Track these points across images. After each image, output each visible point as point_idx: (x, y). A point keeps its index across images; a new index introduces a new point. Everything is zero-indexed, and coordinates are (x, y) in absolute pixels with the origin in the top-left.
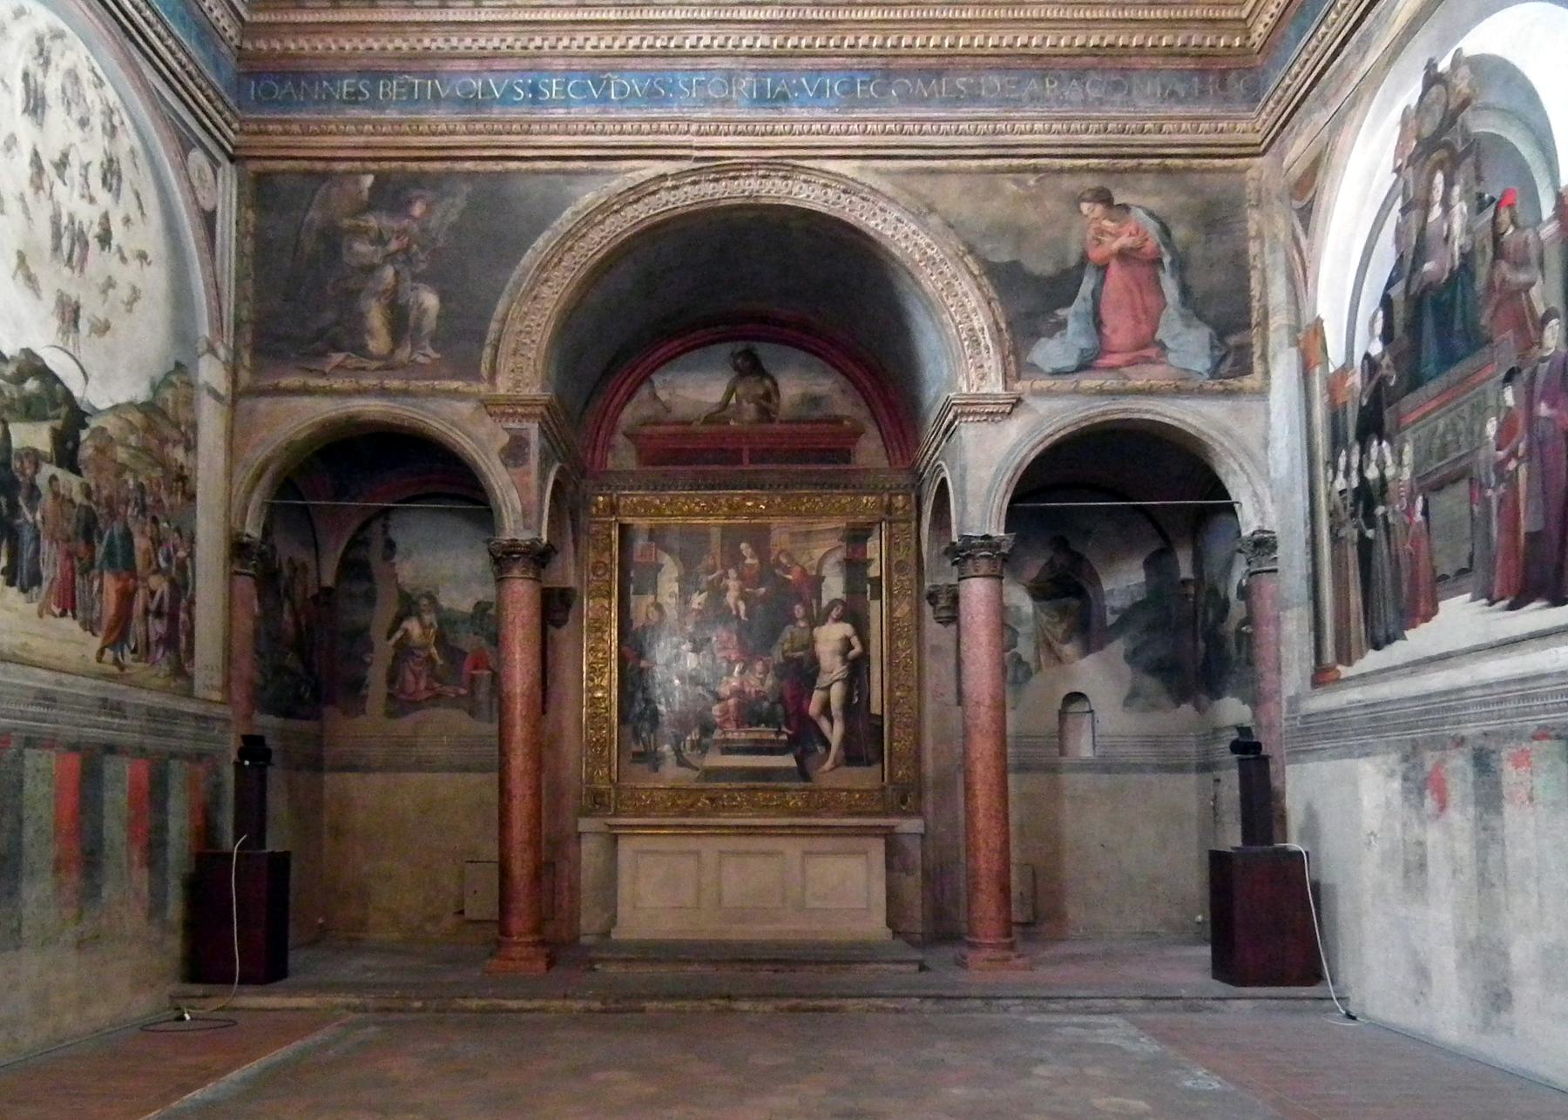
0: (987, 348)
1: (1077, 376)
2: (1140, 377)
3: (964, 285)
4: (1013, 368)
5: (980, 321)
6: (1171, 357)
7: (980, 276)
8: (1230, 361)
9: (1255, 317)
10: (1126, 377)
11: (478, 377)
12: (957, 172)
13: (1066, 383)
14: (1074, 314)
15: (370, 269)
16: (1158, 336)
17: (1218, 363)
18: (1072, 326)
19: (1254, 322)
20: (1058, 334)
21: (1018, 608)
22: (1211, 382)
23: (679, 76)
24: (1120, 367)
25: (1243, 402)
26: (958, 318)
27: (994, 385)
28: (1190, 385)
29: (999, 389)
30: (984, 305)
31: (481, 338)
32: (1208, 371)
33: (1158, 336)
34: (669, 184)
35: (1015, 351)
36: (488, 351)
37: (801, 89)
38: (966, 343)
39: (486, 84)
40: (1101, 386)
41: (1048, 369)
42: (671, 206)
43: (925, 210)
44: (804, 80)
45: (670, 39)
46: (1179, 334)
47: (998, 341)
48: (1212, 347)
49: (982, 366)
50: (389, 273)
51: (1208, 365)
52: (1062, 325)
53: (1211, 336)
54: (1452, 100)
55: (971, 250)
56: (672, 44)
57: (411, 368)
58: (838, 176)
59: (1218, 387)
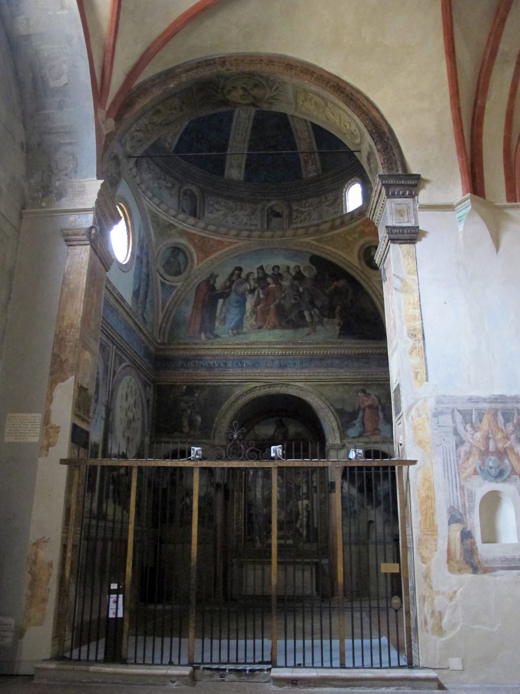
2: (374, 438)
3: (330, 414)
4: (343, 436)
5: (334, 424)
6: (382, 433)
11: (209, 438)
12: (328, 385)
13: (357, 440)
14: (357, 422)
15: (184, 410)
18: (357, 425)
27: (338, 442)
29: (339, 442)
33: (379, 427)
34: (258, 388)
36: (213, 432)
37: (290, 363)
41: (351, 436)
52: (354, 425)
58: (299, 387)
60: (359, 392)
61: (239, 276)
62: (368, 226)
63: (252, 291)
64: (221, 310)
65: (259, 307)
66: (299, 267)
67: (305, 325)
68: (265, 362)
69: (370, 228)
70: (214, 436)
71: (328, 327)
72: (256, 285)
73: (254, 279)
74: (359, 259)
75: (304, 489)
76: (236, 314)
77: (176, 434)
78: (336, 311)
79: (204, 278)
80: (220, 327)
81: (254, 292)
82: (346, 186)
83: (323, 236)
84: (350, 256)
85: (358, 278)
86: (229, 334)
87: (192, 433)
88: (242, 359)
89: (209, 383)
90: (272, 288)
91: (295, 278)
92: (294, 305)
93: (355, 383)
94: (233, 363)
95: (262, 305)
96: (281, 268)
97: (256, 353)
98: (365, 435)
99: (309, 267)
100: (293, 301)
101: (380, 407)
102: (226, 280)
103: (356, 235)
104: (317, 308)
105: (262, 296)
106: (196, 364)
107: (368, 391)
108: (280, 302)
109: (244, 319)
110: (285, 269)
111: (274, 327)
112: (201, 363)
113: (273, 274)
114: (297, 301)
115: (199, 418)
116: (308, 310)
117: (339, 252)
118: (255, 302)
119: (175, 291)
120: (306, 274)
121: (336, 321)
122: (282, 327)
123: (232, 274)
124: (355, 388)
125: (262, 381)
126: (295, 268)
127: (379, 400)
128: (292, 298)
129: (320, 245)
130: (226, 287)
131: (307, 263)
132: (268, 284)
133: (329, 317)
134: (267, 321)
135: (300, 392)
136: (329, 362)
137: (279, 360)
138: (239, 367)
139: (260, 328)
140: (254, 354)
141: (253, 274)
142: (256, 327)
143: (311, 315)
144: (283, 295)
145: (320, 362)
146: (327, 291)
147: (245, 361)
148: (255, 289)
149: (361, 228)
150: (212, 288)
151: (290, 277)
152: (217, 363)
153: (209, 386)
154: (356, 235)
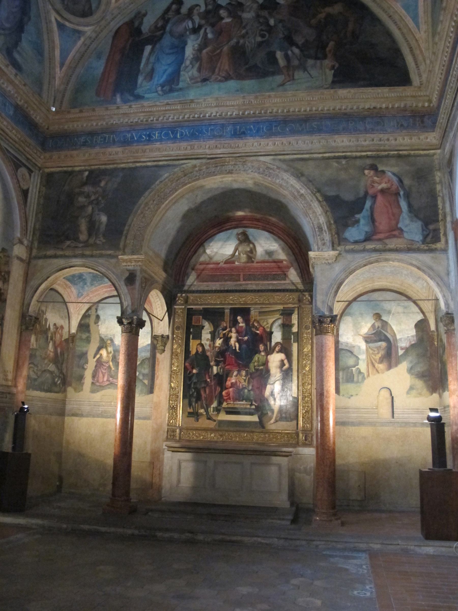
5: (322, 220)
6: (405, 235)
7: (323, 201)
9: (440, 217)
14: (363, 217)
15: (83, 207)
16: (400, 225)
17: (425, 237)
18: (362, 222)
19: (440, 219)
20: (356, 226)
21: (359, 347)
22: (423, 246)
23: (204, 127)
25: (438, 255)
26: (313, 219)
28: (414, 247)
30: (324, 214)
31: (121, 233)
32: (421, 241)
33: (400, 225)
35: (338, 233)
36: (123, 238)
37: (251, 130)
38: (317, 230)
39: (132, 135)
40: (375, 248)
41: (352, 241)
42: (197, 177)
43: (300, 175)
44: (252, 126)
45: (201, 114)
46: (409, 225)
48: (423, 230)
49: (323, 240)
50: (90, 209)
51: (421, 238)
52: (358, 221)
53: (422, 225)
55: (319, 191)
56: (201, 116)
57: (95, 246)
59: (426, 248)
60: (364, 169)
61: (178, 12)
63: (195, 31)
64: (148, 59)
65: (204, 51)
67: (277, 71)
68: (211, 130)
70: (125, 246)
71: (314, 72)
72: (203, 22)
73: (199, 14)
75: (277, 337)
76: (169, 64)
77: (68, 243)
78: (328, 49)
79: (127, 19)
80: (145, 83)
81: (199, 32)
86: (157, 92)
87: (91, 241)
88: (175, 128)
89: (123, 166)
90: (226, 23)
92: (260, 44)
93: (358, 154)
94: (161, 133)
95: (209, 48)
97: (196, 116)
98: (375, 237)
100: (259, 39)
101: (402, 193)
102: (159, 18)
104: (298, 47)
105: (210, 36)
106: (105, 138)
107: (380, 168)
109: (181, 69)
111: (227, 78)
112: (113, 137)
113: (229, 4)
114: (264, 39)
115: (104, 219)
118: (199, 45)
119: (82, 39)
122: (240, 77)
123: (168, 10)
124: (358, 162)
125: (203, 156)
127: (401, 181)
130: (157, 28)
132: (222, 19)
133: (317, 58)
134: (217, 70)
135: (266, 171)
136: (314, 124)
137: (234, 124)
138: (169, 139)
139: (205, 80)
140: (194, 117)
141: (198, 8)
142: (199, 80)
144: (244, 31)
145: (301, 125)
146: (313, 22)
147: (179, 129)
148: (200, 27)
150: (138, 31)
151: (255, 6)
152: (136, 136)
153: (123, 169)
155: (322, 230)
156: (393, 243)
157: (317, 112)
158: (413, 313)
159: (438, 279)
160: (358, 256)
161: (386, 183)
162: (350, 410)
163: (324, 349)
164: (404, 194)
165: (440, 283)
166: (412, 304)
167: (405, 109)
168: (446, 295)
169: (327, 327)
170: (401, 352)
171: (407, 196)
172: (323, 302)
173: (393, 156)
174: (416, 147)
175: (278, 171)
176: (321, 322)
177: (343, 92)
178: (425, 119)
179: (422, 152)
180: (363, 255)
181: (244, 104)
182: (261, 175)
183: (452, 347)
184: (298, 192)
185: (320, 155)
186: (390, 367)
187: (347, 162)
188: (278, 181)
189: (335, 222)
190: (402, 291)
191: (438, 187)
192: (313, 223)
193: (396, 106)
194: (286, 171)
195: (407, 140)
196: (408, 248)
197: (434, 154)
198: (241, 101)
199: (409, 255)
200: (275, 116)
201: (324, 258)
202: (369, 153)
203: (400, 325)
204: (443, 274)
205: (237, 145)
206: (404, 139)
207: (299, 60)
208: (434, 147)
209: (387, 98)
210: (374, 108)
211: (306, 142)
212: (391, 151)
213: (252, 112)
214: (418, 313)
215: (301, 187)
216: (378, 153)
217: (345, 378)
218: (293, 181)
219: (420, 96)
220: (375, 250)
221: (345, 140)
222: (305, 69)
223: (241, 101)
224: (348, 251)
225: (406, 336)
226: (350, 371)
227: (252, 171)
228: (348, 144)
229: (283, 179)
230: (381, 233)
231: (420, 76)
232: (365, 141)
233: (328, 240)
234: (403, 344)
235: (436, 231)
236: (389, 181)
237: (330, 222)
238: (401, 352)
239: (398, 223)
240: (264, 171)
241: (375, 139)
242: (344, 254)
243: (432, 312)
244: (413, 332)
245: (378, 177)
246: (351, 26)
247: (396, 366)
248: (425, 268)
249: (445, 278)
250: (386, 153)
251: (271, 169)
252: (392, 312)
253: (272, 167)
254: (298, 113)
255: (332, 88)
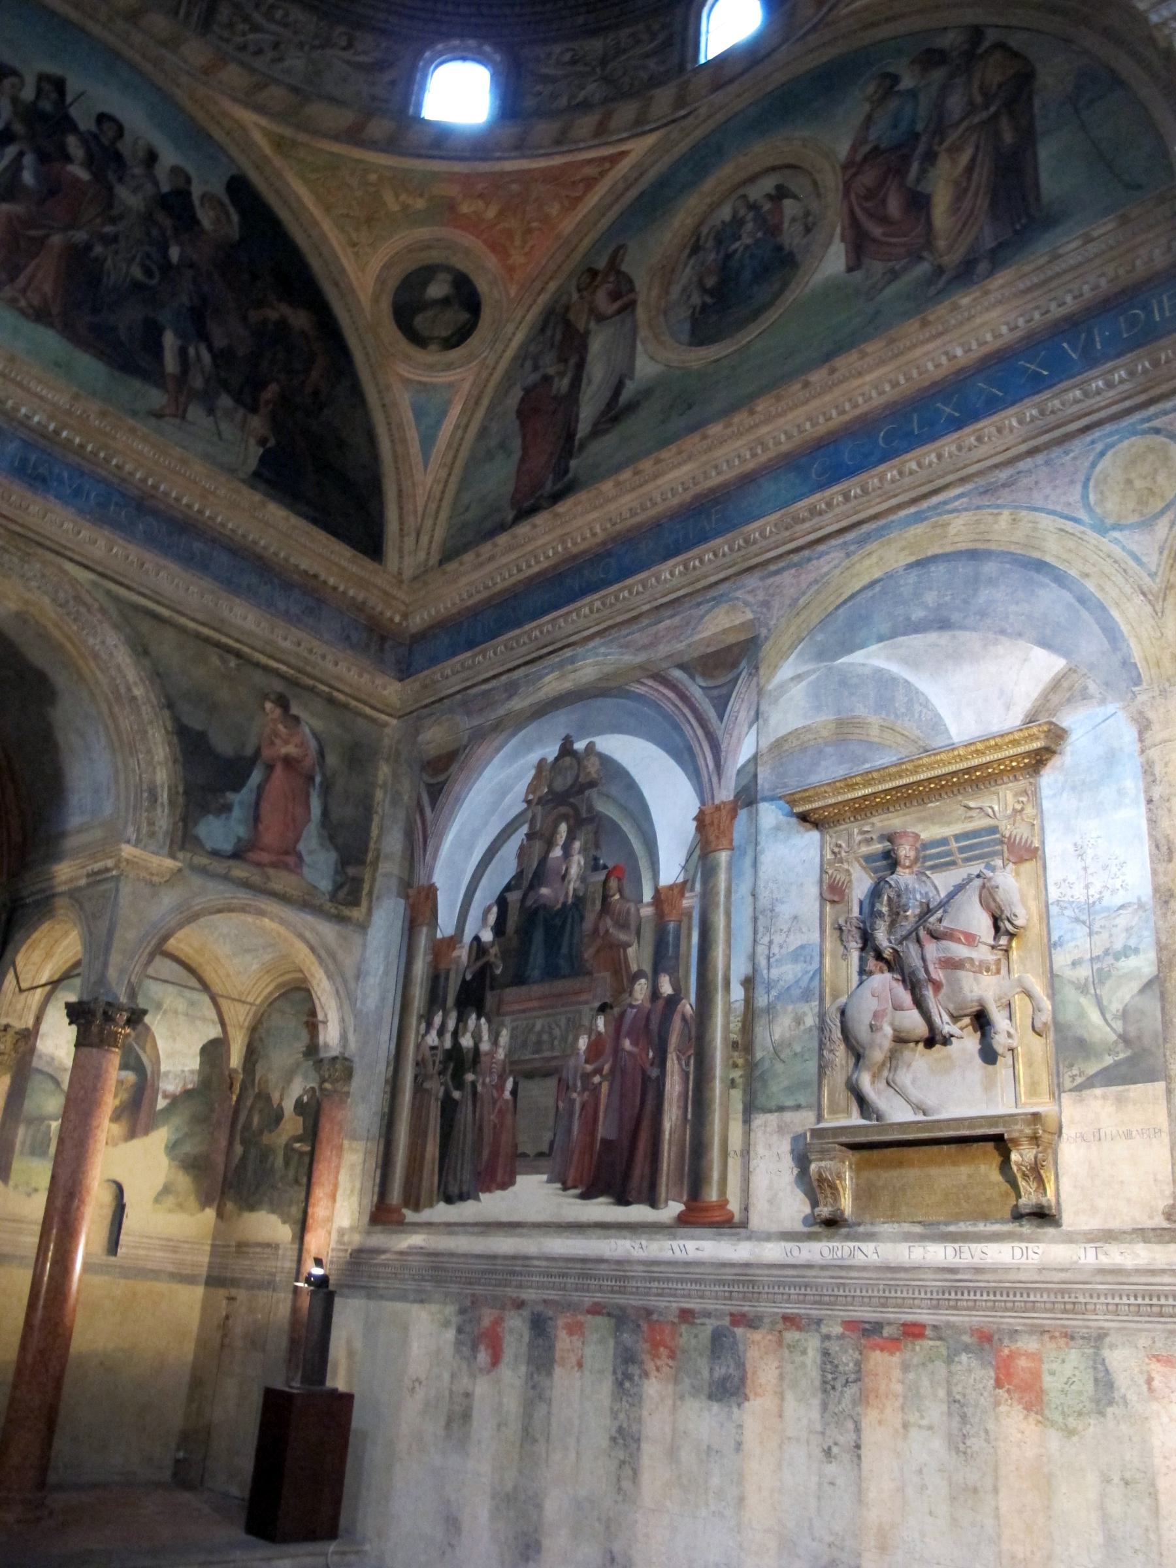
0: (162, 805)
1: (231, 862)
5: (162, 776)
6: (306, 870)
8: (345, 889)
10: (268, 878)
13: (218, 866)
14: (240, 799)
17: (338, 887)
18: (237, 813)
20: (224, 816)
22: (329, 904)
24: (265, 865)
26: (143, 765)
33: (301, 847)
35: (185, 819)
37: (60, 481)
40: (247, 878)
41: (209, 845)
43: (140, 649)
44: (66, 474)
47: (172, 802)
48: (337, 872)
49: (154, 824)
51: (330, 888)
52: (227, 808)
54: (582, 775)
55: (170, 705)
59: (333, 911)
60: (266, 697)
62: (481, 196)
66: (188, 180)
67: (153, 375)
69: (480, 204)
71: (224, 426)
74: (381, 281)
82: (440, 47)
83: (302, 137)
84: (357, 254)
85: (352, 342)
91: (164, 202)
92: (137, 286)
93: (264, 660)
96: (128, 138)
98: (254, 856)
99: (222, 204)
100: (137, 272)
101: (318, 779)
103: (420, 204)
104: (210, 349)
107: (295, 710)
108: (88, 247)
110: (141, 154)
111: (40, 316)
113: (95, 137)
116: (180, 334)
117: (327, 225)
120: (206, 218)
121: (257, 423)
124: (258, 677)
126: (176, 171)
127: (321, 754)
128: (138, 260)
129: (278, 162)
131: (218, 187)
133: (239, 400)
134: (22, 281)
136: (197, 546)
137: (26, 444)
143: (183, 353)
144: (109, 229)
146: (254, 316)
149: (453, 190)
151: (149, 188)
154: (420, 204)
155: (156, 801)
156: (281, 881)
157: (210, 523)
158: (204, 1019)
159: (339, 980)
160: (211, 885)
161: (296, 746)
162: (24, 1226)
163: (99, 1085)
164: (321, 784)
165: (341, 991)
166: (205, 999)
167: (361, 607)
168: (346, 1019)
169: (117, 1033)
170: (161, 1103)
171: (327, 789)
172: (122, 971)
173: (319, 694)
174: (364, 697)
175: (99, 616)
176: (108, 1018)
177: (276, 512)
178: (387, 645)
179: (368, 710)
180: (221, 887)
181: (69, 413)
182: (59, 609)
183: (336, 1128)
184: (129, 689)
185: (192, 625)
186: (132, 1134)
187: (238, 665)
188: (91, 641)
189: (186, 793)
190: (194, 965)
191: (379, 794)
192: (140, 776)
193: (351, 593)
194: (116, 627)
195: (352, 676)
196: (304, 900)
197: (386, 725)
198: (63, 400)
199: (302, 915)
200: (123, 480)
201: (147, 869)
202: (283, 668)
203: (174, 1040)
204: (350, 973)
205: (24, 504)
206: (349, 670)
207: (207, 381)
208: (389, 710)
209: (344, 569)
210: (315, 576)
211: (176, 581)
212: (322, 682)
213: (77, 440)
214: (213, 1022)
215: (137, 680)
216: (299, 675)
217: (28, 1142)
218: (123, 657)
219: (394, 598)
220: (246, 885)
221: (250, 617)
222: (211, 411)
223: (63, 400)
224: (194, 868)
225: (180, 1068)
226: (43, 1128)
227: (39, 588)
228: (253, 628)
229: (103, 642)
230: (262, 849)
231: (401, 557)
232: (285, 639)
233: (165, 828)
234: (170, 1086)
235: (357, 882)
236: (302, 744)
237: (176, 787)
238: (161, 1103)
239: (297, 840)
240: (67, 602)
241: (303, 644)
242: (187, 872)
243: (241, 1027)
244: (193, 1063)
245: (286, 727)
246: (315, 374)
247: (146, 1132)
248: (323, 953)
249: (352, 985)
250: (311, 682)
251: (85, 604)
252: (165, 1006)
253: (89, 600)
254: (172, 502)
255: (253, 487)
